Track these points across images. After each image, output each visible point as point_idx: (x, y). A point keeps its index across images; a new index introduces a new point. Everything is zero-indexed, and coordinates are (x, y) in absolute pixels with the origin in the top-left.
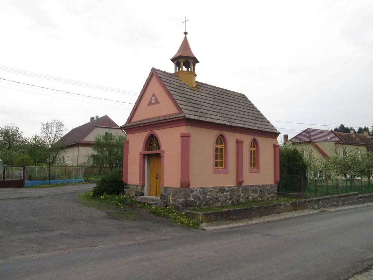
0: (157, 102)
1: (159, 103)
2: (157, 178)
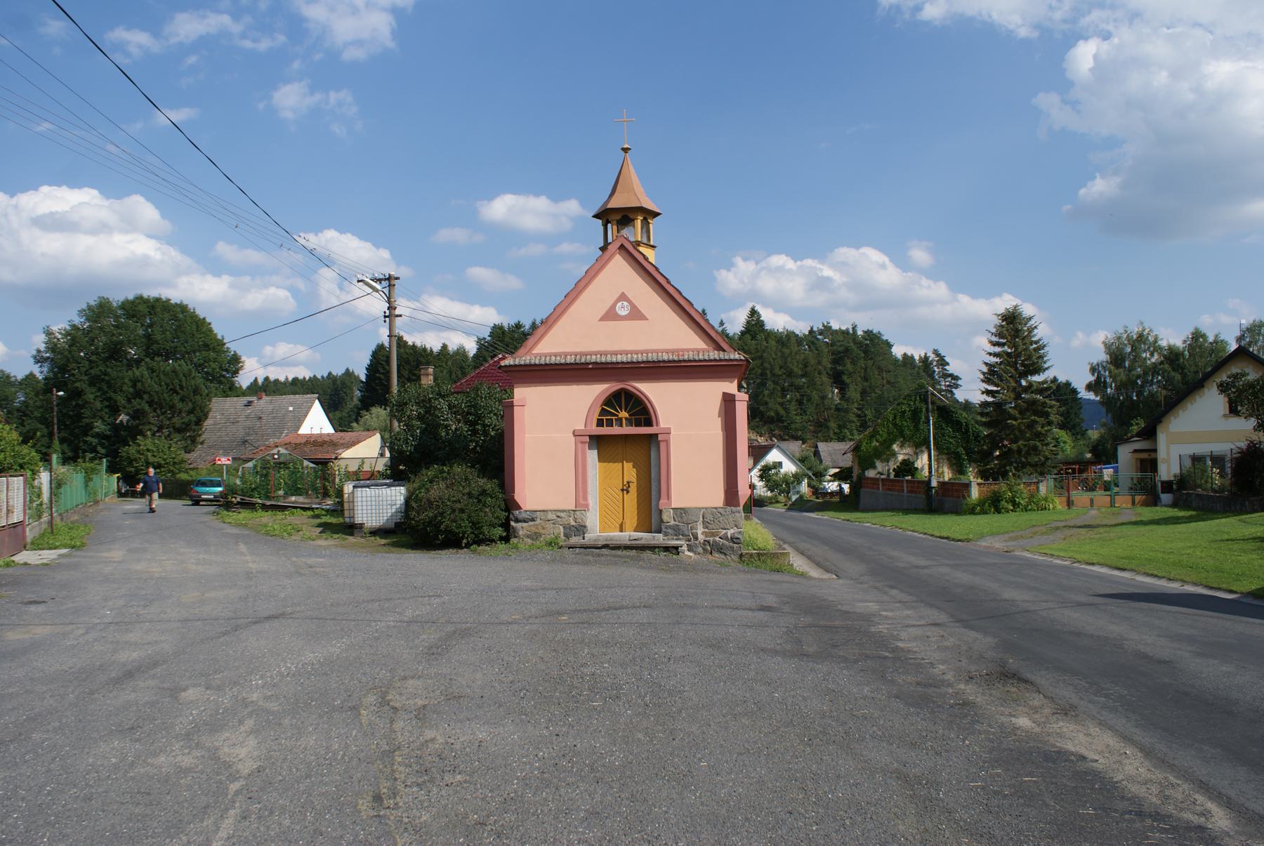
0: (635, 314)
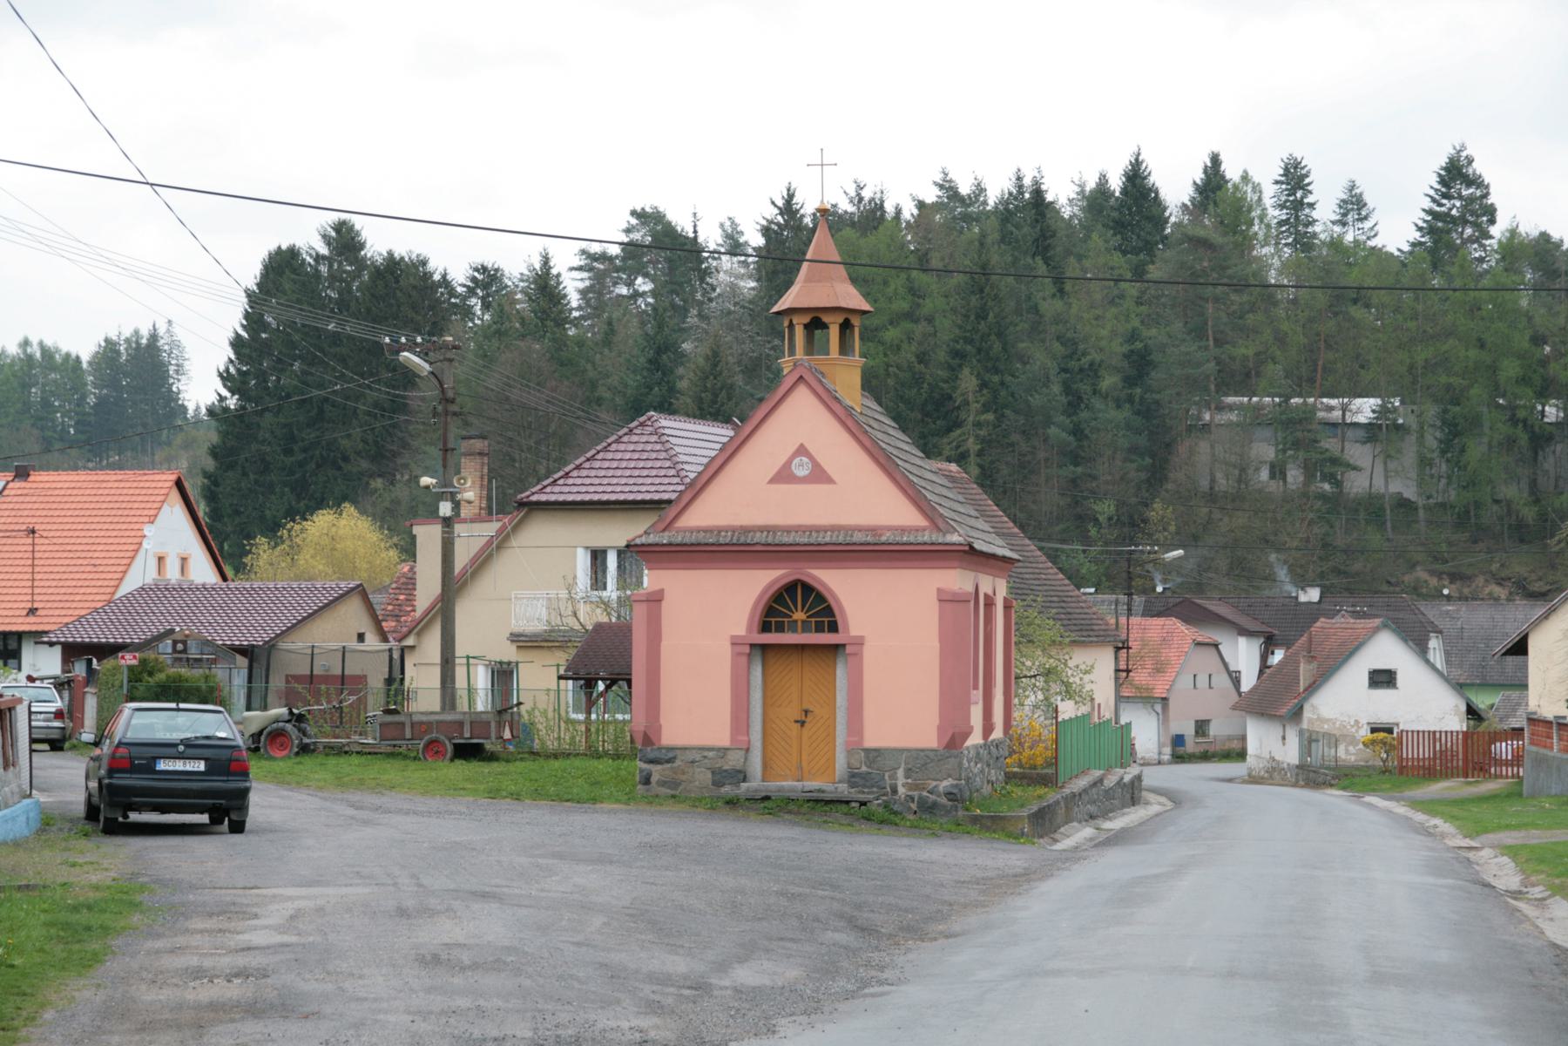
0: (819, 475)
1: (829, 480)
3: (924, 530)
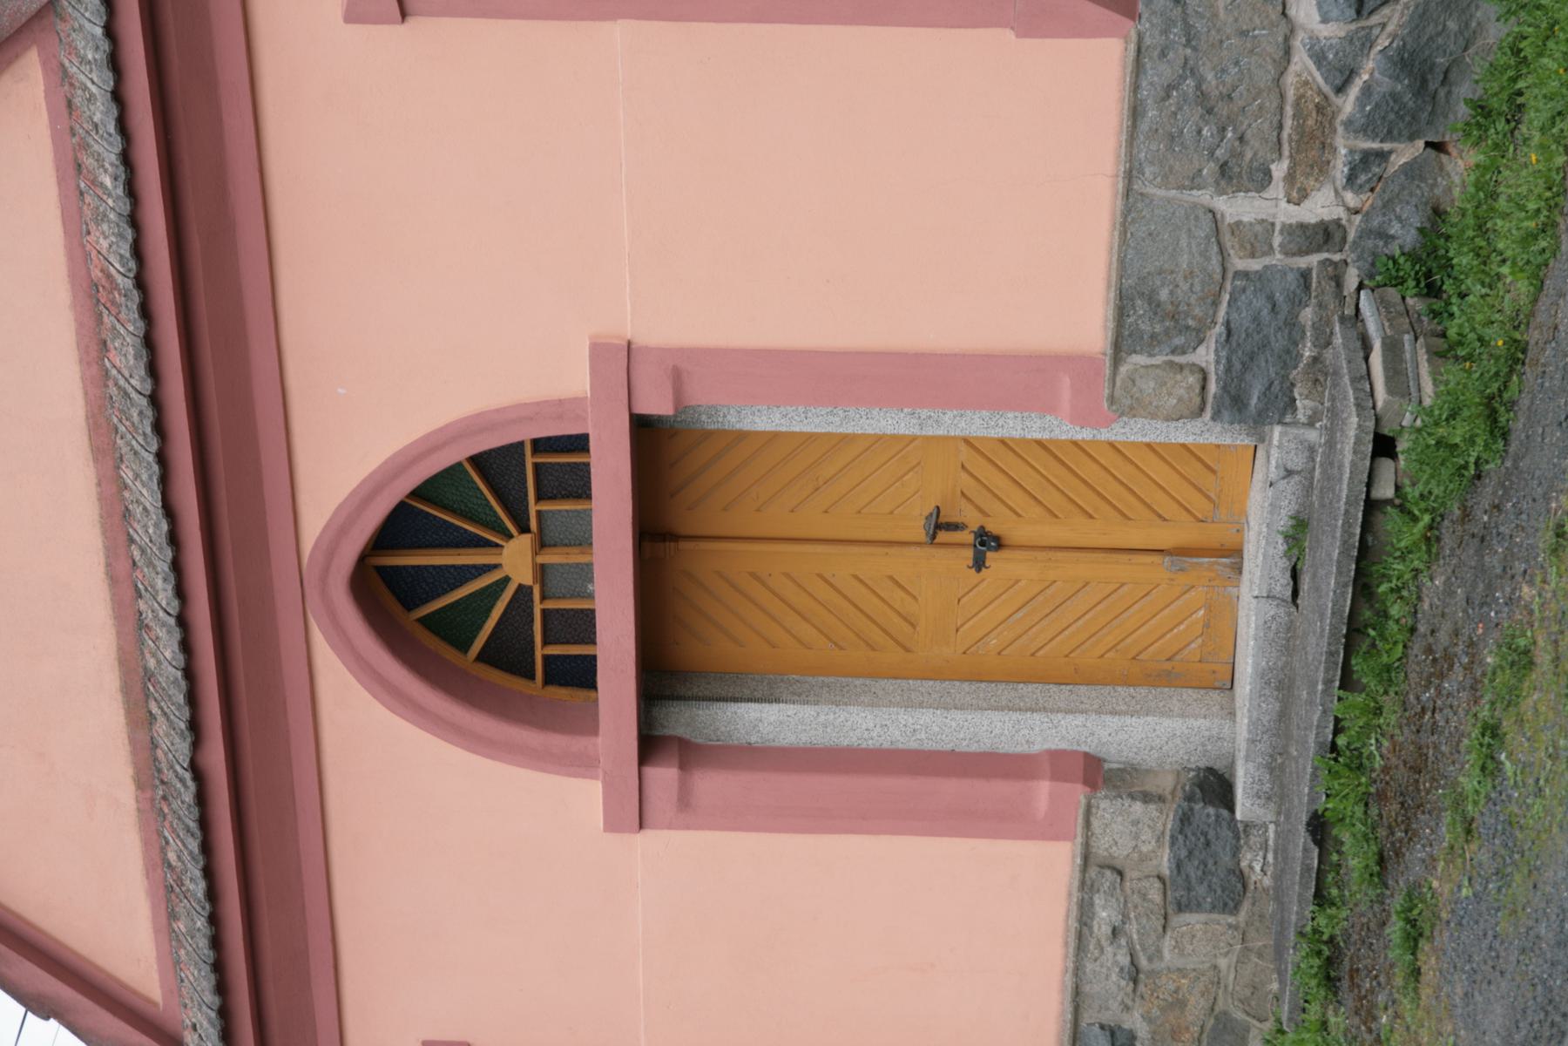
2: (988, 542)
3: (60, 77)
